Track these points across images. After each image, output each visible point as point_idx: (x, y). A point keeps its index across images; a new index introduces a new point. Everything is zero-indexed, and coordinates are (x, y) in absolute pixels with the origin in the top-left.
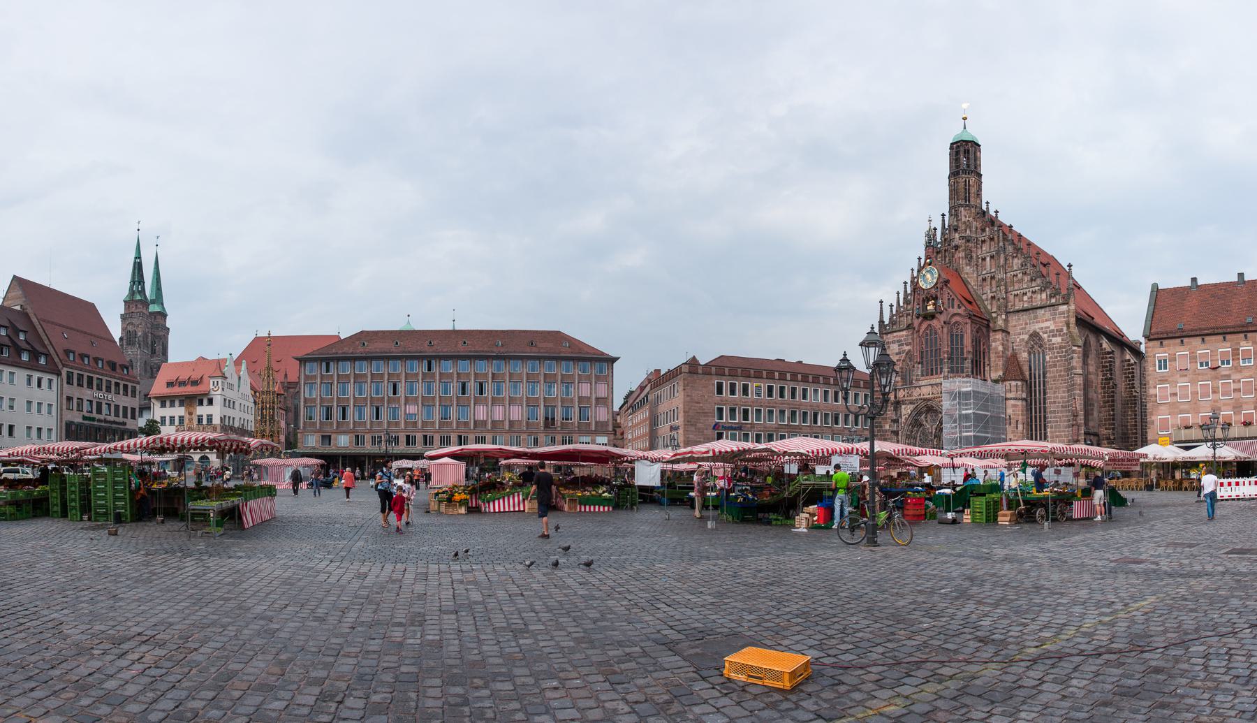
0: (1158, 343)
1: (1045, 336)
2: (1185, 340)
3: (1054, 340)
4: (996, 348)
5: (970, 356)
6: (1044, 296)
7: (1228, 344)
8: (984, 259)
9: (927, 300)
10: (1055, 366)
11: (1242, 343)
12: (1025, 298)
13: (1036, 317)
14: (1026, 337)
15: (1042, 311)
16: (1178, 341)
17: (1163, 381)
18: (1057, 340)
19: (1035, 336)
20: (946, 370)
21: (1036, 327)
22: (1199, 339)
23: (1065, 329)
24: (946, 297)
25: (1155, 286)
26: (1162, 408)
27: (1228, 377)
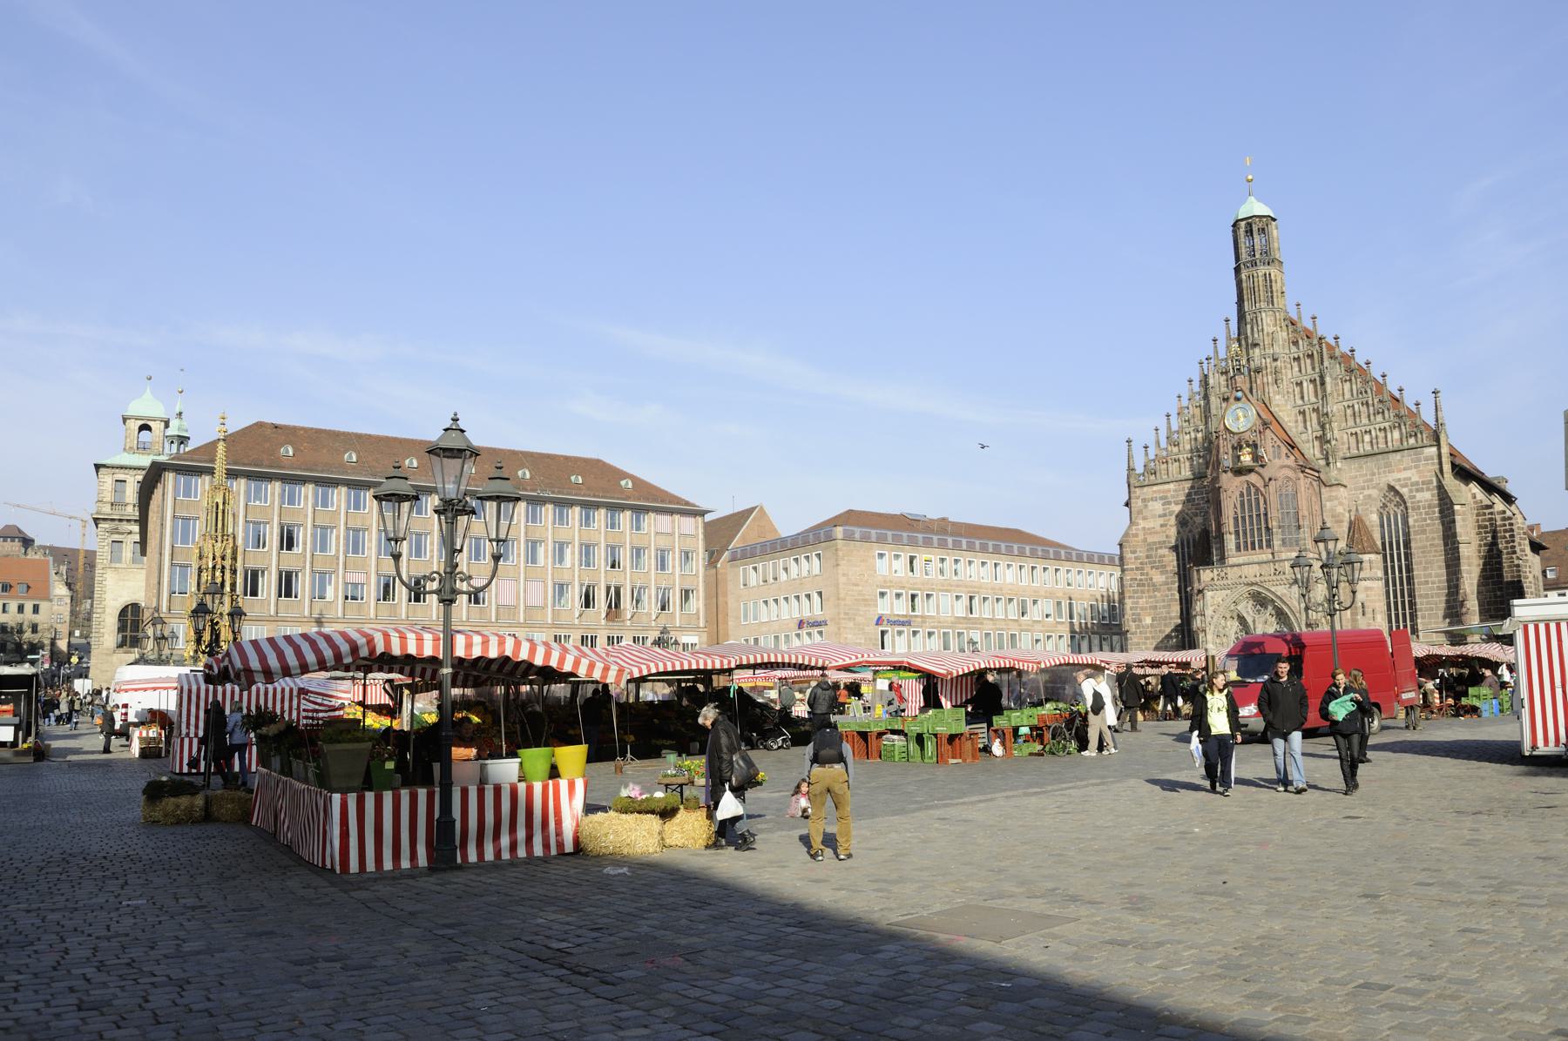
1: (1404, 491)
3: (1419, 496)
4: (1332, 510)
5: (1306, 523)
6: (1396, 434)
8: (1300, 384)
9: (1238, 447)
10: (1424, 532)
12: (1367, 438)
13: (1388, 465)
14: (1374, 493)
20: (1277, 543)
21: (1391, 478)
24: (1269, 444)
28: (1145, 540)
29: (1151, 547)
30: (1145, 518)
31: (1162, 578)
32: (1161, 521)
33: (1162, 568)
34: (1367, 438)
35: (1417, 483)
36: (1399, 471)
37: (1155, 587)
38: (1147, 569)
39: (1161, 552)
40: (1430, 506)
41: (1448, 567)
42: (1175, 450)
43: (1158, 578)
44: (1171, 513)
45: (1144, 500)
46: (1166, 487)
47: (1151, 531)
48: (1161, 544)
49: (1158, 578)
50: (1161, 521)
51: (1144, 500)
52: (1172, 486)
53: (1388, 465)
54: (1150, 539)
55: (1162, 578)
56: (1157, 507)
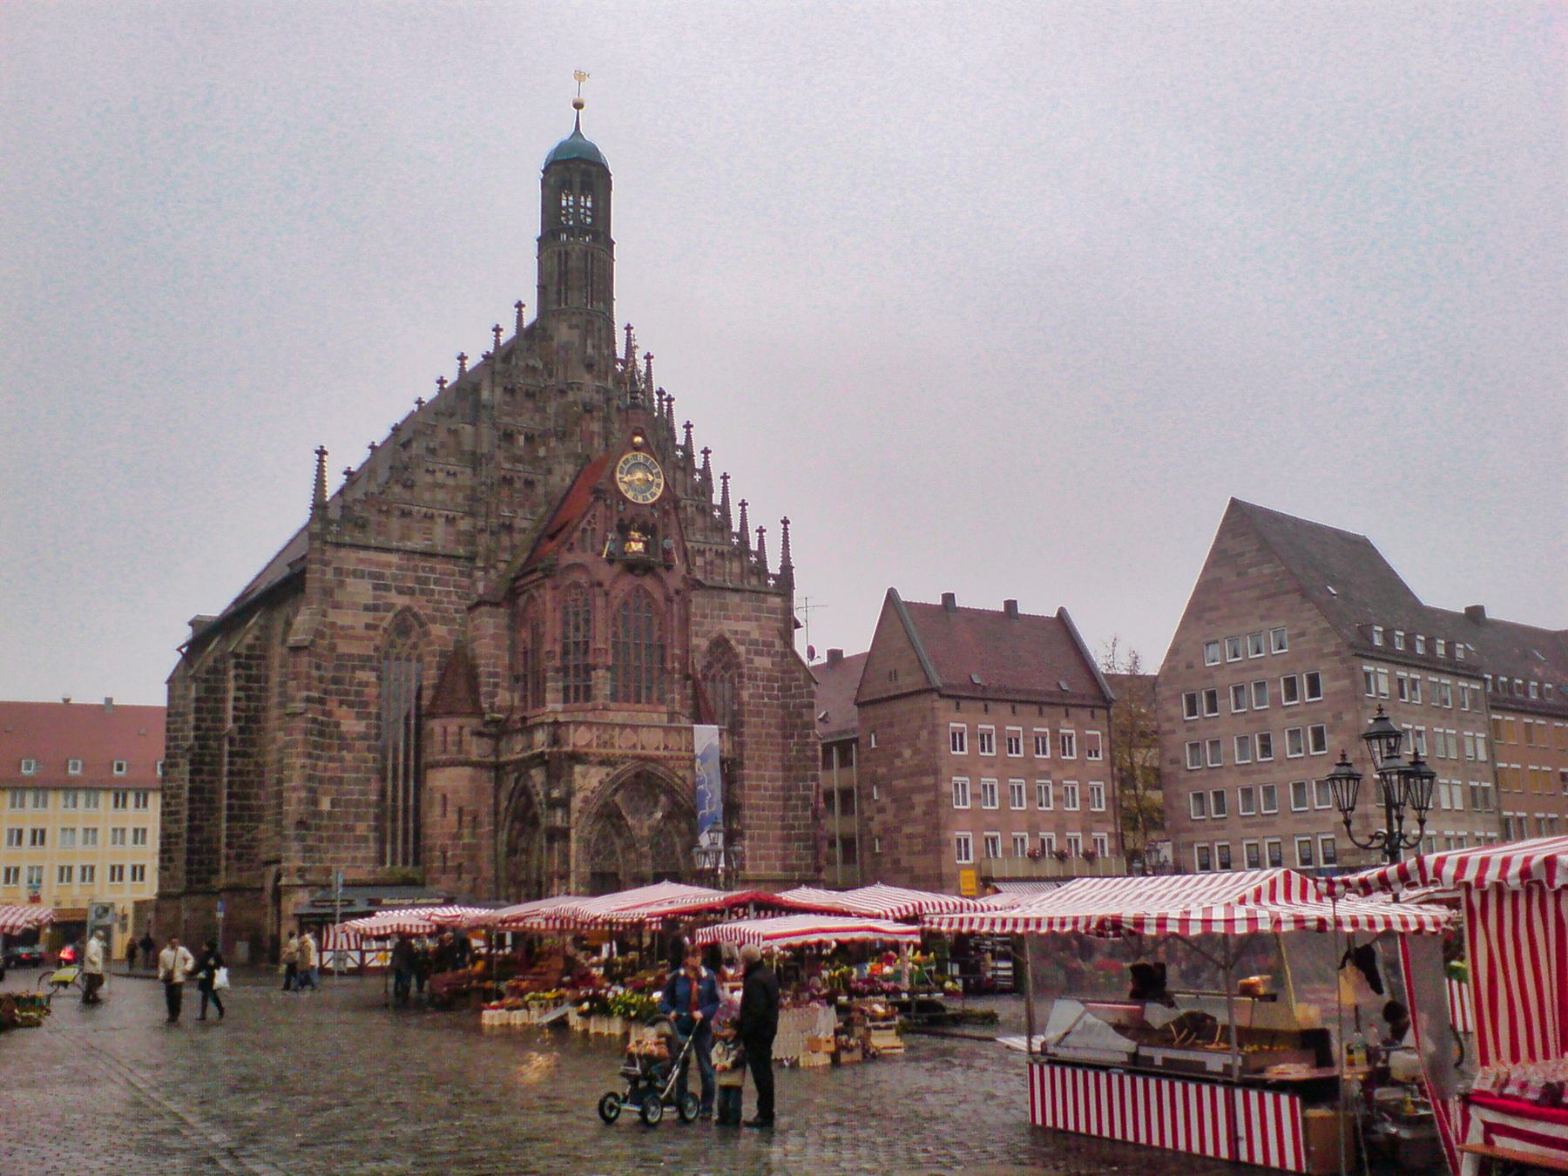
0: (952, 703)
1: (741, 649)
2: (991, 705)
7: (1046, 721)
10: (759, 714)
11: (1064, 722)
13: (723, 607)
15: (736, 598)
16: (981, 705)
17: (960, 772)
18: (763, 662)
19: (721, 645)
21: (727, 627)
22: (1007, 708)
23: (779, 645)
25: (892, 596)
26: (960, 817)
27: (1046, 775)
28: (333, 648)
29: (343, 662)
30: (337, 606)
31: (360, 727)
32: (368, 618)
33: (359, 706)
34: (699, 561)
35: (754, 642)
36: (737, 619)
37: (344, 743)
38: (332, 704)
39: (361, 675)
40: (769, 680)
41: (787, 768)
42: (407, 495)
43: (351, 725)
44: (389, 607)
45: (339, 571)
46: (385, 557)
47: (345, 633)
48: (364, 662)
49: (351, 725)
50: (368, 618)
51: (339, 571)
52: (394, 558)
53: (723, 607)
54: (343, 648)
55: (360, 727)
56: (361, 591)
